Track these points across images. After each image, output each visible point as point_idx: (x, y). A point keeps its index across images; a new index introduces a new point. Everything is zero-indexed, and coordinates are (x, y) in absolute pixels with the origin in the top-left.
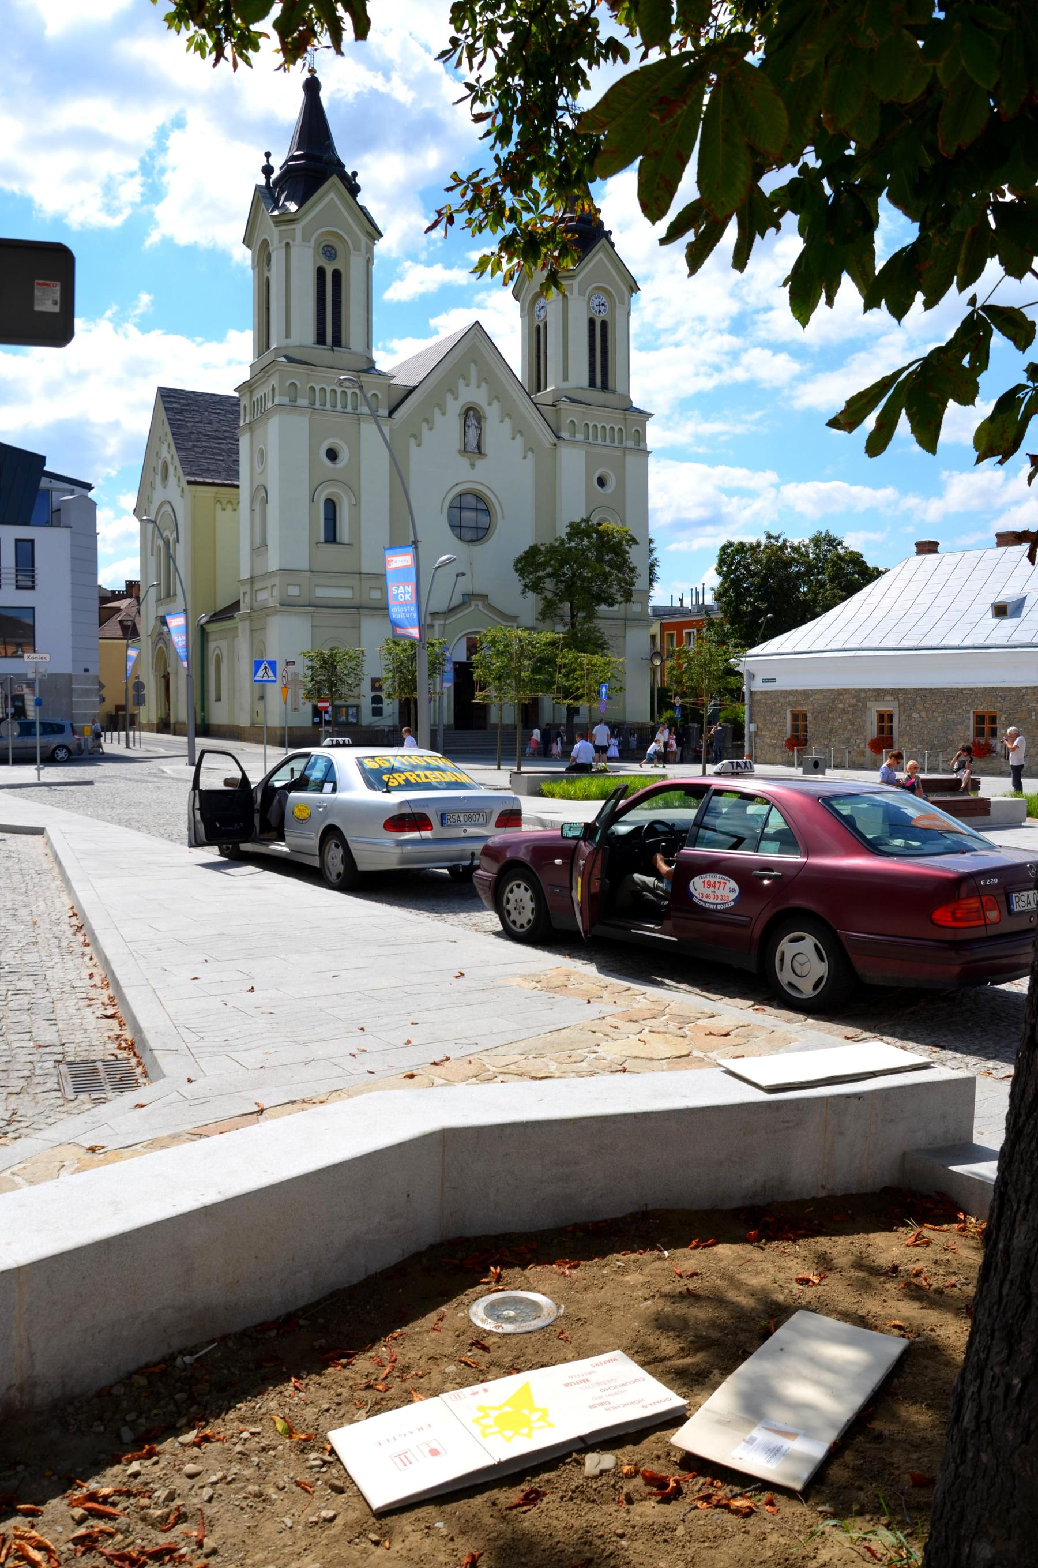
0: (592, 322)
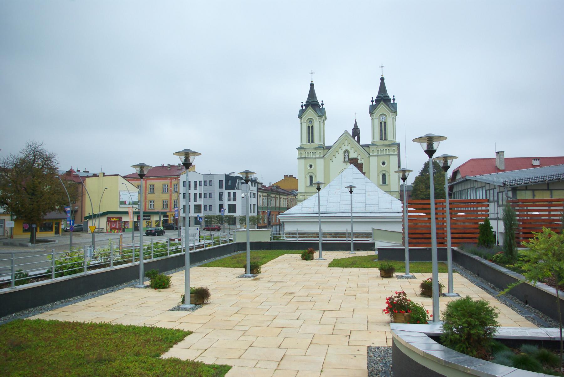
0: (381, 123)
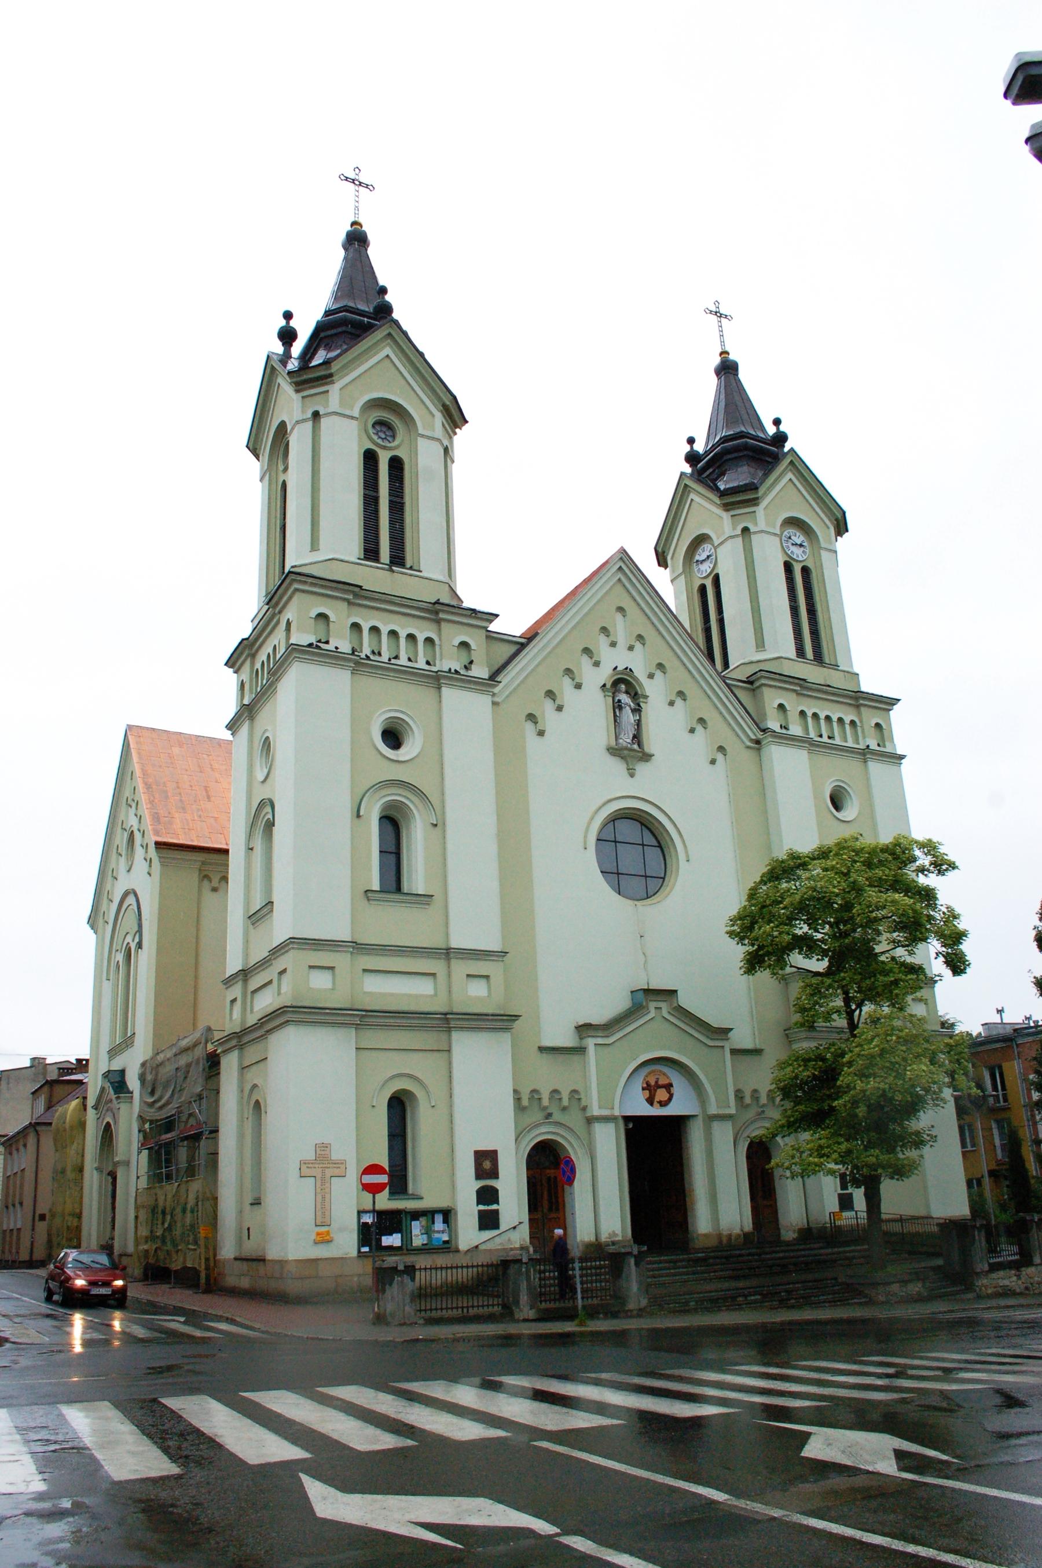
0: (788, 567)
